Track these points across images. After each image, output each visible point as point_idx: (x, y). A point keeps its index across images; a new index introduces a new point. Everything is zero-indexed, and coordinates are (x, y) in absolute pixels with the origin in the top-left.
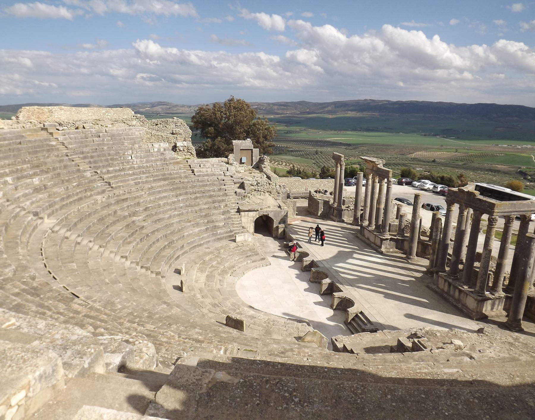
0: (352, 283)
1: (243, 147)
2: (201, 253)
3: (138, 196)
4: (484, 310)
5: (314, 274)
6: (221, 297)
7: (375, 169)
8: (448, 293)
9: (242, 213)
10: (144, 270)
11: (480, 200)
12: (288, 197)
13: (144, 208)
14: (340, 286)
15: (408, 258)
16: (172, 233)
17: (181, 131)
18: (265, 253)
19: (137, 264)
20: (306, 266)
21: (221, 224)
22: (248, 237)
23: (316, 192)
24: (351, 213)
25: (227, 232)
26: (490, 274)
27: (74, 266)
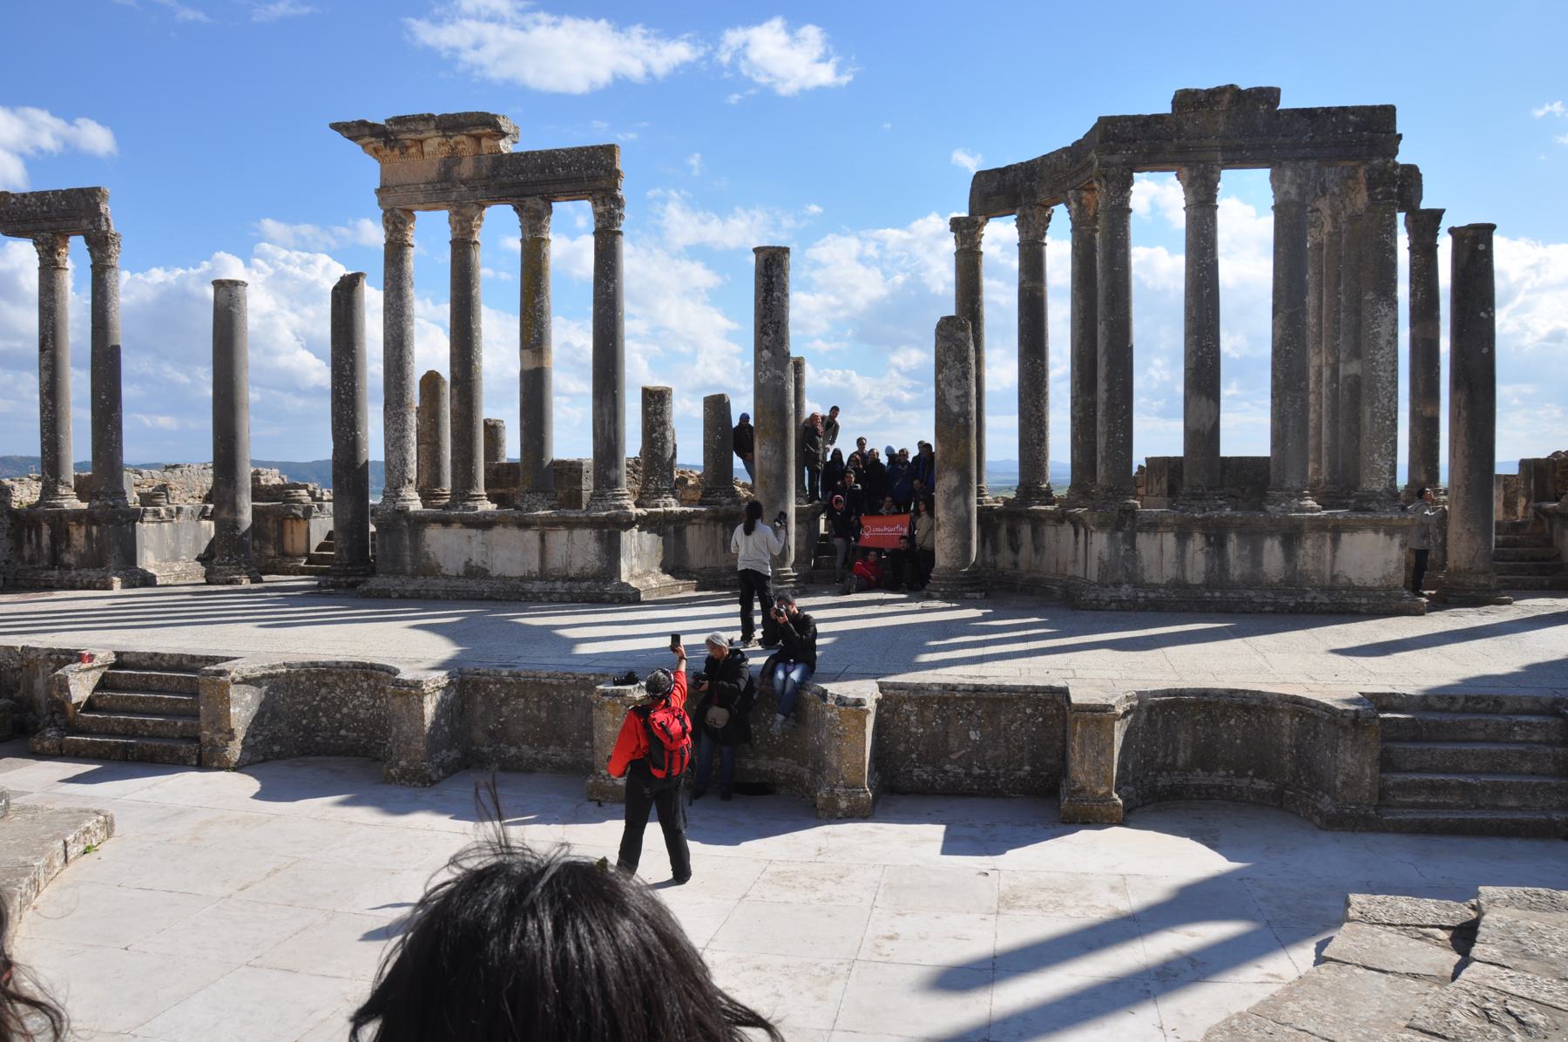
7: (466, 169)
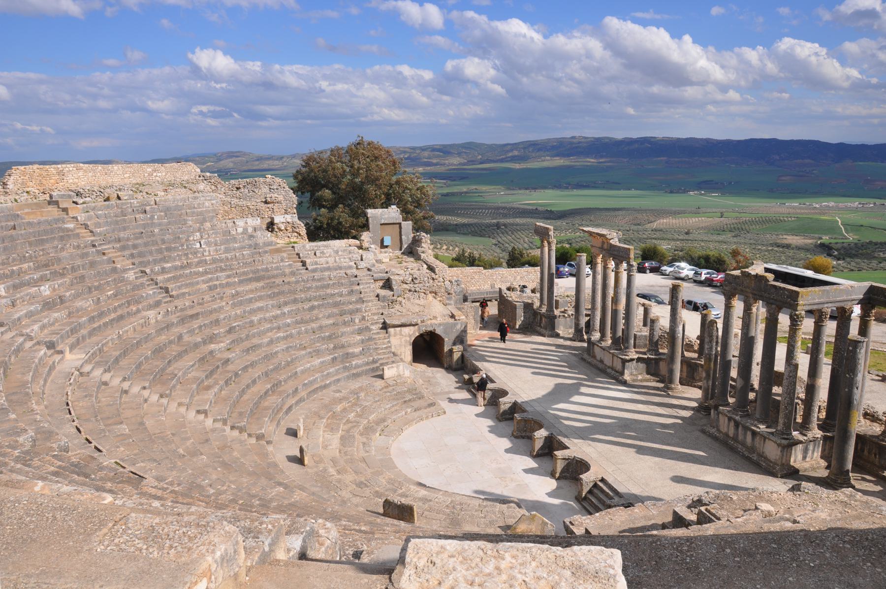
0: (583, 434)
1: (385, 219)
2: (327, 401)
3: (215, 309)
4: (792, 460)
5: (519, 424)
6: (369, 471)
7: (605, 246)
8: (735, 438)
9: (391, 330)
10: (236, 433)
11: (775, 286)
12: (465, 300)
13: (227, 328)
14: (565, 440)
15: (667, 388)
16: (277, 369)
17: (281, 198)
18: (434, 394)
19: (225, 422)
20: (505, 412)
21: (357, 350)
22: (404, 369)
23: (509, 289)
24: (571, 322)
25: (368, 364)
26: (797, 403)
27: (125, 429)
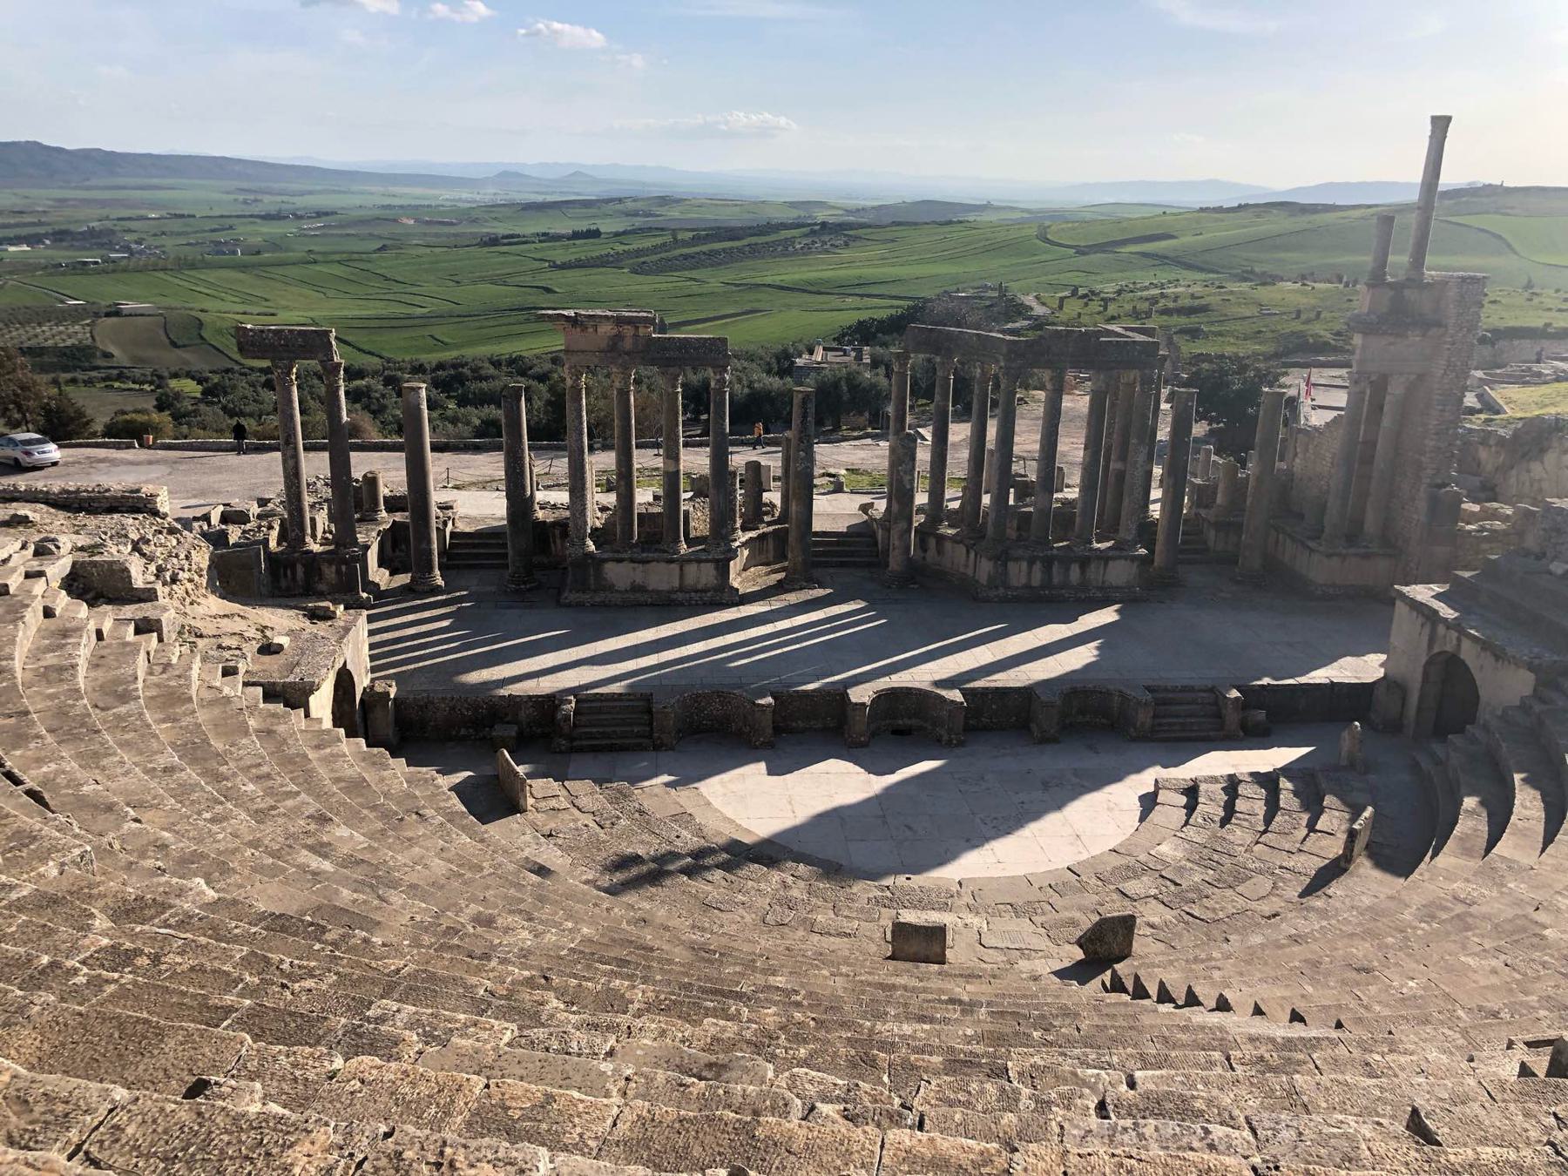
7: (628, 344)
